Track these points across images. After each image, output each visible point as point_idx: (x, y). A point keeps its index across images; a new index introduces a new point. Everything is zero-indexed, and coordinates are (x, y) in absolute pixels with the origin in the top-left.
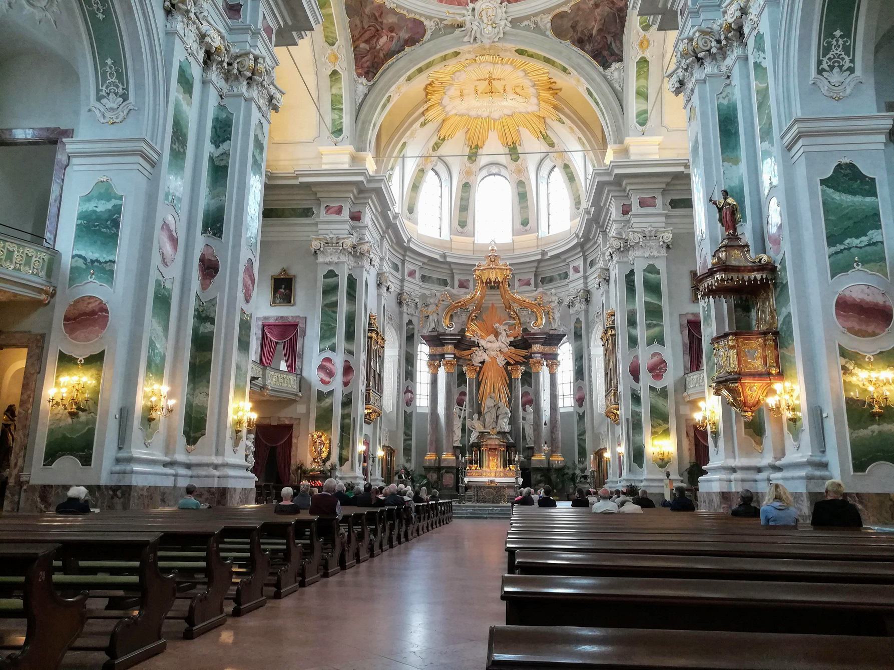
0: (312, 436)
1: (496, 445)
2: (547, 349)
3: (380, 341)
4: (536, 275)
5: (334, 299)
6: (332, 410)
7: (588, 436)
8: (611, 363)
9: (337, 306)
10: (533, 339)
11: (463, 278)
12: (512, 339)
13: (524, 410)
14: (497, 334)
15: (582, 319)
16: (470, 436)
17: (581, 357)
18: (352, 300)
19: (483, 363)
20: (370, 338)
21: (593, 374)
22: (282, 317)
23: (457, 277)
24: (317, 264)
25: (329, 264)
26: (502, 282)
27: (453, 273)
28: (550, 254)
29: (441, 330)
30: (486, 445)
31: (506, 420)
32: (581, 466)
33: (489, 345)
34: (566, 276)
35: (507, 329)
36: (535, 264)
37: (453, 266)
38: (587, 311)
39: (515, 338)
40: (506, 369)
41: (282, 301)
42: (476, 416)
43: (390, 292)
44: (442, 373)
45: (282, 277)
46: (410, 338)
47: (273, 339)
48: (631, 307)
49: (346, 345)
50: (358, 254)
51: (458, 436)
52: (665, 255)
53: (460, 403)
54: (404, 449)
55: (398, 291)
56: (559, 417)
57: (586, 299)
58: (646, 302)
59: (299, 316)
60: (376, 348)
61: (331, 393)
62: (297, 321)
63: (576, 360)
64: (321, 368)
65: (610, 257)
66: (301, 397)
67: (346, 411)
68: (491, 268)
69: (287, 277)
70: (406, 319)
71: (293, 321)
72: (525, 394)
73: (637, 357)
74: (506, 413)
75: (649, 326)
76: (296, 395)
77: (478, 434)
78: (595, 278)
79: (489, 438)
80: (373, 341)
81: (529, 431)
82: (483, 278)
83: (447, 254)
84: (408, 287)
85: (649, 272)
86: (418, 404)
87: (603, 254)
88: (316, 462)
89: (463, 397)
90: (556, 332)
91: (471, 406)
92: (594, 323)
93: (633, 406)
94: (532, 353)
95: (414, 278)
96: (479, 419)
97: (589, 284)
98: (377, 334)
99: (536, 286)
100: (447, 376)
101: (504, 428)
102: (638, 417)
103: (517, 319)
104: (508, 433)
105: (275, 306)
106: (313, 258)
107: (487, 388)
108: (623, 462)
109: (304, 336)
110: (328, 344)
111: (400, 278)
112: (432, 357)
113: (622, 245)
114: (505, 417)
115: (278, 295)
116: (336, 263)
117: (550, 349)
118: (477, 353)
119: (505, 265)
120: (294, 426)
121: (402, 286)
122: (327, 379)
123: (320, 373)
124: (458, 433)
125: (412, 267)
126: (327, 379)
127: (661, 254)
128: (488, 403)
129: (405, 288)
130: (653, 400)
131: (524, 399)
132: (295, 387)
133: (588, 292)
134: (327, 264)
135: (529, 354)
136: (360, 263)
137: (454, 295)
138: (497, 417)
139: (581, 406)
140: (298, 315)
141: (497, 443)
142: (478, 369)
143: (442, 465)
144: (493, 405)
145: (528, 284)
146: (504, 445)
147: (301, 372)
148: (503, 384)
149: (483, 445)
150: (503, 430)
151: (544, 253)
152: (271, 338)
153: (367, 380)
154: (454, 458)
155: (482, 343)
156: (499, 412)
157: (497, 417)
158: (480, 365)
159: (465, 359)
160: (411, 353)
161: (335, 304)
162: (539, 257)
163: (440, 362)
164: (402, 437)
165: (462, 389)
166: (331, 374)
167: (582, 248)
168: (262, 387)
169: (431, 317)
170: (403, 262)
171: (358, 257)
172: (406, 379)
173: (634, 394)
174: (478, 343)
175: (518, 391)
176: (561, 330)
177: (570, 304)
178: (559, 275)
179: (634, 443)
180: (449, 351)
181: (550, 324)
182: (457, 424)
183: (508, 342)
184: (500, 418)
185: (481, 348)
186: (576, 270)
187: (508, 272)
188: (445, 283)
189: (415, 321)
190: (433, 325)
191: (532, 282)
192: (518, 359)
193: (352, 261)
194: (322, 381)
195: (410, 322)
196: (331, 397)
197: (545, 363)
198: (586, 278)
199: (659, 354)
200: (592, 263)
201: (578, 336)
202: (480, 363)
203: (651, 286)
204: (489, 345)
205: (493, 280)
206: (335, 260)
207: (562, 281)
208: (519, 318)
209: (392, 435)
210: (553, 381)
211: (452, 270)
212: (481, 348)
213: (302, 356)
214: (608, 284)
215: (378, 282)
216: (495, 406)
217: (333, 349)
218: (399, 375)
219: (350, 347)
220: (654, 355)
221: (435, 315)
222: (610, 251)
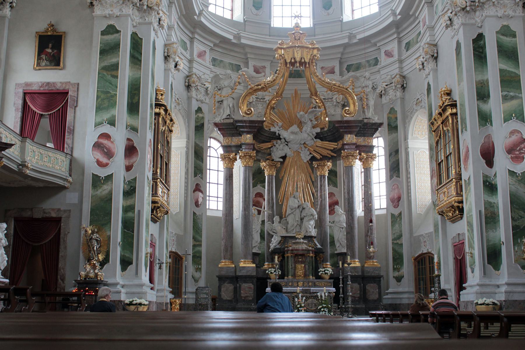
0: (86, 231)
1: (303, 250)
2: (361, 141)
3: (168, 122)
4: (341, 63)
5: (114, 60)
6: (111, 199)
7: (405, 240)
8: (452, 147)
9: (117, 69)
10: (346, 127)
11: (259, 64)
12: (318, 130)
13: (332, 212)
14: (300, 124)
15: (398, 109)
16: (269, 241)
17: (397, 152)
18: (136, 64)
19: (284, 158)
20: (158, 115)
21: (411, 170)
22: (48, 84)
23: (251, 63)
24: (93, 18)
25: (110, 17)
26: (309, 63)
27: (247, 59)
28: (359, 37)
29: (237, 118)
30: (292, 250)
31: (312, 223)
32: (397, 274)
33: (292, 137)
34: (376, 61)
35: (313, 119)
36: (341, 50)
37: (248, 50)
38: (403, 99)
39: (321, 129)
40: (311, 165)
41: (48, 63)
42: (276, 218)
43: (178, 70)
44: (239, 167)
45: (49, 34)
46: (199, 128)
47: (37, 111)
48: (480, 78)
49: (129, 118)
50: (145, 7)
51: (257, 242)
52: (521, 14)
53: (258, 204)
54: (194, 257)
55: (187, 73)
56: (374, 219)
57: (403, 86)
58: (501, 70)
59: (69, 82)
60: (164, 129)
61: (109, 178)
62: (67, 88)
63: (390, 155)
64: (97, 146)
65: (449, 22)
66: (71, 183)
67: (129, 202)
68: (295, 47)
69: (55, 34)
70: (195, 106)
71: (62, 88)
72: (331, 195)
73: (489, 137)
74: (312, 215)
75: (505, 98)
76: (65, 180)
77: (280, 239)
78: (417, 58)
79: (294, 243)
80: (160, 119)
81: (340, 236)
82: (286, 57)
83: (241, 34)
84: (197, 69)
85: (503, 35)
86: (208, 207)
87: (432, 28)
88: (90, 264)
89: (260, 199)
90: (371, 122)
91: (271, 207)
92: (413, 112)
93: (486, 196)
94: (344, 145)
95: (204, 60)
96: (280, 222)
97: (405, 69)
98: (166, 110)
99: (341, 74)
100: (245, 171)
101: (310, 232)
102: (492, 209)
103: (323, 109)
104: (315, 237)
105: (39, 70)
106: (88, 11)
107: (288, 186)
108: (473, 264)
109: (75, 107)
110: (106, 116)
111: (189, 58)
112: (227, 148)
113: (468, 4)
114: (311, 219)
115: (43, 56)
116: (117, 16)
117: (364, 140)
118: (277, 145)
119: (312, 44)
120: (62, 220)
121: (190, 68)
122: (104, 160)
123: (95, 152)
124: (257, 237)
125: (202, 48)
126: (104, 160)
127: (517, 14)
128: (293, 203)
129: (194, 70)
130: (513, 187)
131: (331, 201)
132: (63, 169)
133: (404, 77)
134: (105, 17)
135: (340, 146)
136: (147, 19)
137: (252, 77)
138: (302, 219)
139: (396, 206)
140: (68, 81)
141: (304, 249)
142: (279, 165)
143: (239, 274)
144: (297, 206)
145: (332, 72)
146: (312, 251)
147: (72, 152)
148: (307, 182)
149: (288, 250)
150: (309, 235)
151: (351, 36)
152: (34, 109)
153: (153, 166)
154: (254, 265)
155: (284, 134)
156: (304, 214)
157: (302, 219)
158: (282, 160)
159: (264, 153)
160: (201, 145)
161: (115, 67)
162: (346, 41)
163: (236, 155)
164: (190, 242)
165: (259, 189)
166: (109, 154)
167: (397, 28)
168: (20, 165)
169: (225, 103)
170: (192, 40)
171: (145, 11)
172: (195, 175)
173: (487, 181)
174: (279, 135)
175: (324, 191)
176: (376, 119)
177: (383, 92)
178: (368, 61)
179: (488, 241)
180: (248, 141)
181: (364, 112)
182: (256, 228)
183: (314, 133)
184: (305, 220)
185: (283, 140)
186: (389, 54)
187: (315, 52)
188: (238, 68)
189: (205, 108)
190: (228, 112)
191: (337, 70)
192: (325, 153)
193: (136, 16)
194: (100, 164)
195: (199, 110)
196: (110, 183)
197: (358, 158)
198: (401, 61)
199: (519, 132)
200: (408, 46)
201: (393, 128)
202: (281, 158)
203: (506, 51)
204: (292, 137)
205: (298, 59)
206: (117, 12)
207: (371, 68)
208: (325, 108)
209: (180, 240)
210: (367, 177)
211: (246, 54)
212: (283, 140)
213: (72, 132)
214: (436, 62)
215: (166, 54)
216: (299, 207)
217: (112, 123)
218: (187, 170)
219: (132, 122)
220: (512, 133)
221: (230, 100)
222: (449, 14)
